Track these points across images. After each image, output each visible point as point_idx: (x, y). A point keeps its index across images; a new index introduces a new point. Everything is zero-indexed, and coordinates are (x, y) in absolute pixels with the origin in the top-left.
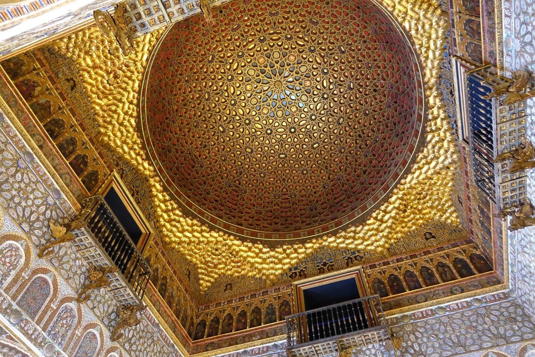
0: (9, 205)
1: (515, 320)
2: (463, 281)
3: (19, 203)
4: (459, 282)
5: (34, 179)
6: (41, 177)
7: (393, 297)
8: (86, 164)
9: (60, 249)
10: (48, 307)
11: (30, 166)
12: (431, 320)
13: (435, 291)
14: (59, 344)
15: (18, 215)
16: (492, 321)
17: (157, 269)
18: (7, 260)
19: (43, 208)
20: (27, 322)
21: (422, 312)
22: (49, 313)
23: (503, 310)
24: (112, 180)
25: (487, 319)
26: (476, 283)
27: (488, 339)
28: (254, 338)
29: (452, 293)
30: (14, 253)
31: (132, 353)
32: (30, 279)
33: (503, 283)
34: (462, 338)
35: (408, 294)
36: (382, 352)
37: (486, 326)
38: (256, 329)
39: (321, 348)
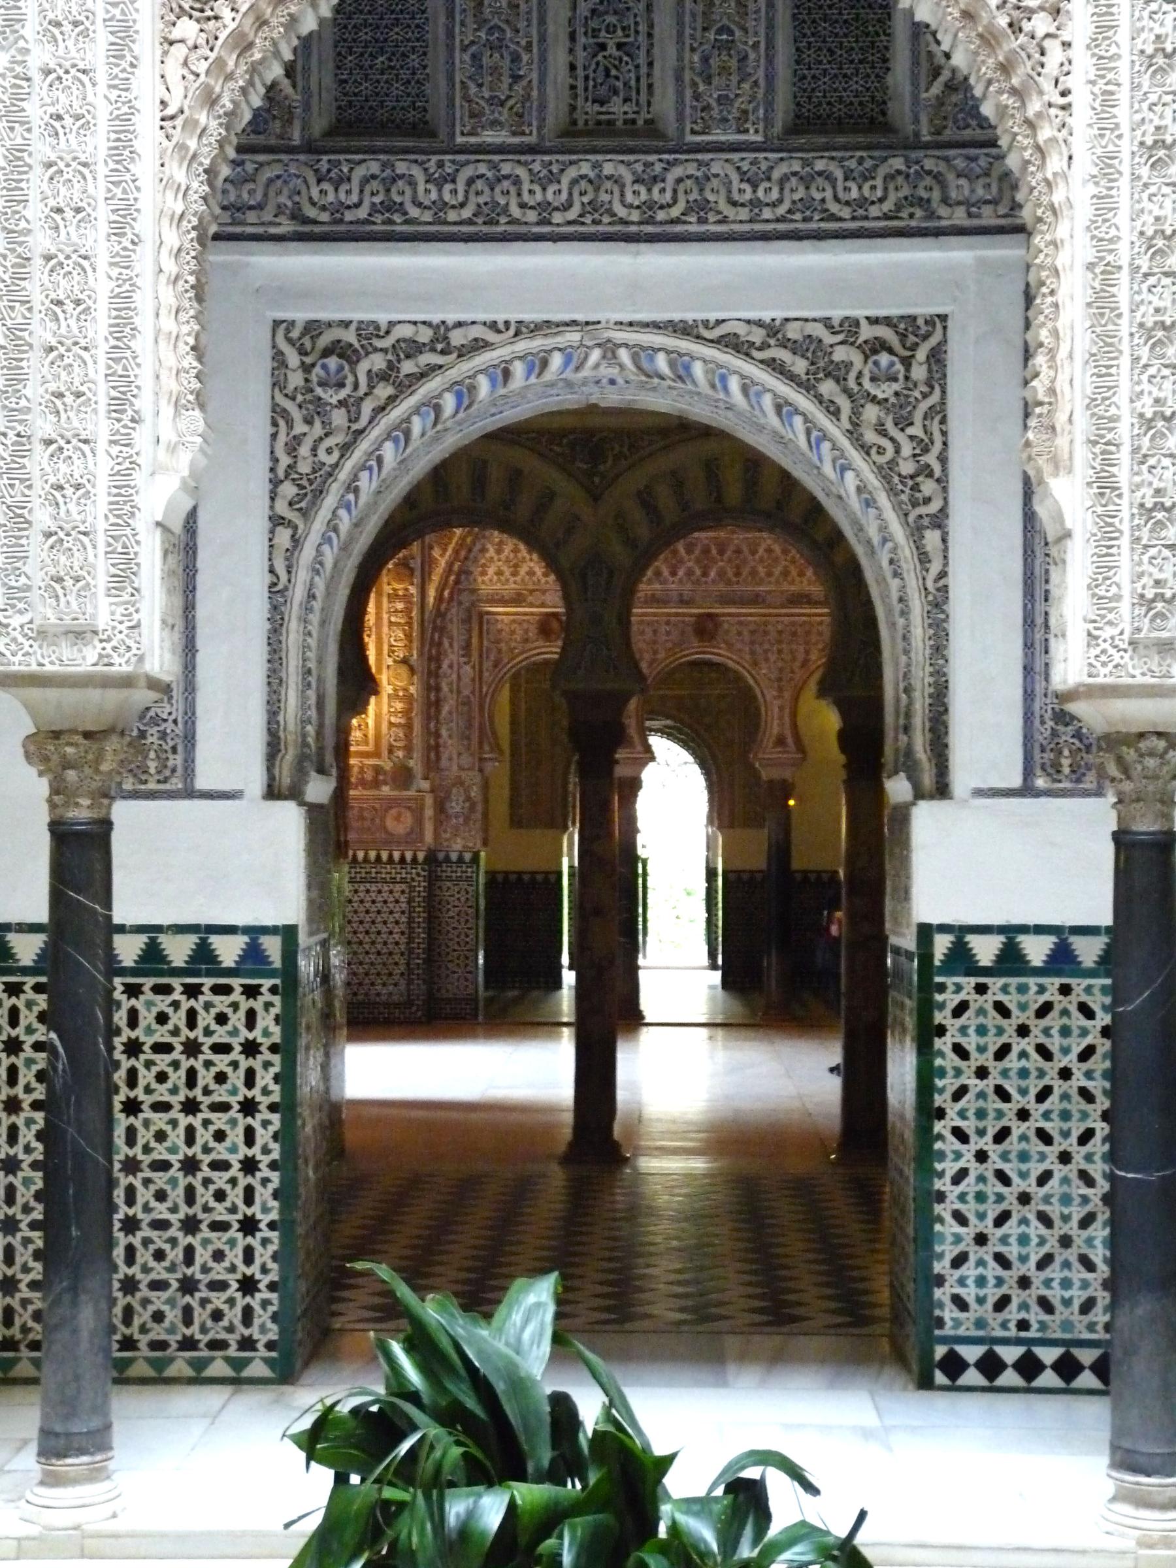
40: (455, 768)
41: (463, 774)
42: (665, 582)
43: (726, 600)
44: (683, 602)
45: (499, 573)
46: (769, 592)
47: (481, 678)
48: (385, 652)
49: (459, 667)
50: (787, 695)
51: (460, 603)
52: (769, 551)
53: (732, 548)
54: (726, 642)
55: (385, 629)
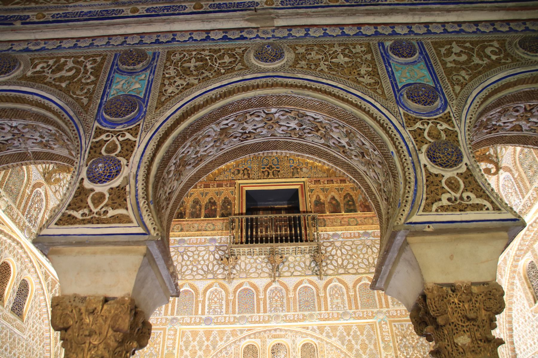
0: (193, 275)
3: (198, 269)
5: (193, 249)
6: (196, 243)
8: (214, 204)
9: (240, 266)
10: (258, 300)
11: (186, 245)
14: (282, 311)
15: (202, 275)
17: (333, 198)
18: (216, 299)
19: (212, 256)
20: (252, 317)
22: (261, 302)
24: (242, 187)
30: (216, 294)
31: (350, 271)
32: (235, 297)
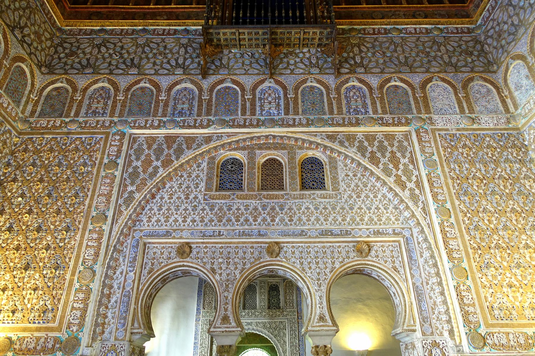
1: (471, 54)
2: (430, 7)
4: (426, 7)
7: (345, 8)
12: (382, 38)
13: (395, 11)
16: (447, 50)
21: (374, 29)
23: (463, 43)
25: (442, 48)
26: (443, 13)
27: (438, 65)
28: (158, 18)
29: (414, 17)
33: (472, 18)
34: (410, 60)
35: (364, 8)
36: (317, 58)
37: (440, 54)
38: (163, 8)
39: (246, 37)
40: (113, 339)
41: (117, 343)
42: (251, 224)
43: (285, 234)
44: (260, 235)
45: (158, 221)
46: (309, 230)
47: (139, 280)
48: (80, 263)
49: (127, 273)
50: (324, 288)
51: (133, 237)
52: (308, 208)
53: (287, 207)
54: (286, 258)
55: (83, 249)
